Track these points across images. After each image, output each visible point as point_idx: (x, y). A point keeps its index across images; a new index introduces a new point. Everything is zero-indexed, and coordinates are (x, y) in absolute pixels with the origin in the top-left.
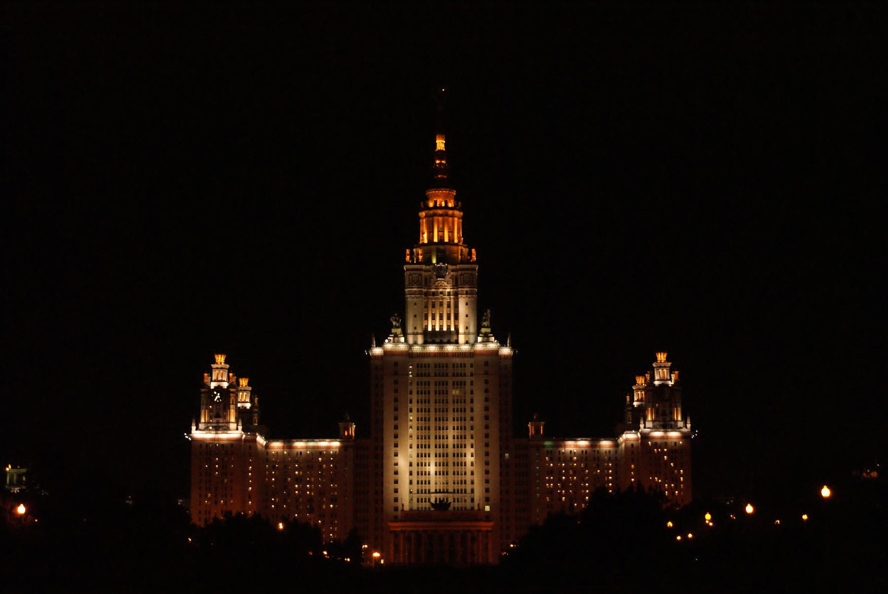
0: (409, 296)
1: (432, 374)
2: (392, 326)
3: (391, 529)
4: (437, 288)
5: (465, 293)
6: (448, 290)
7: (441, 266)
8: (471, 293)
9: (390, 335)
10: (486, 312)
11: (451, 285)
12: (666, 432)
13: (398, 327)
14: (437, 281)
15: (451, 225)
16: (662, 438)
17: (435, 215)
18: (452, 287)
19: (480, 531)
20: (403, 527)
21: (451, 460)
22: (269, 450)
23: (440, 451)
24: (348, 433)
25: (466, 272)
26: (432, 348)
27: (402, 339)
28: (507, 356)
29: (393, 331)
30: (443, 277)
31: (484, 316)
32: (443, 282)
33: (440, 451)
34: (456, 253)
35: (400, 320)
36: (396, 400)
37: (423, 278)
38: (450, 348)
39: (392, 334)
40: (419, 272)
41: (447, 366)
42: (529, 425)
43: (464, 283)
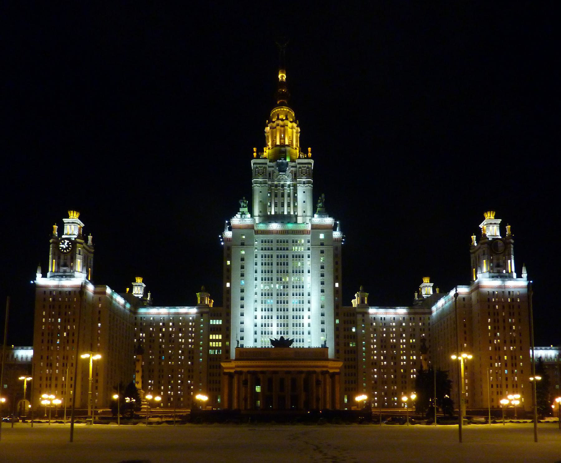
0: (255, 185)
1: (274, 248)
2: (240, 206)
3: (226, 371)
4: (279, 180)
5: (303, 183)
6: (288, 183)
7: (282, 162)
8: (309, 182)
9: (238, 213)
10: (321, 196)
11: (291, 178)
12: (503, 281)
13: (245, 207)
14: (278, 175)
15: (290, 135)
16: (500, 287)
17: (278, 125)
18: (291, 180)
19: (327, 372)
21: (291, 321)
23: (281, 313)
25: (304, 165)
27: (249, 215)
29: (241, 210)
30: (285, 171)
32: (284, 176)
33: (281, 313)
35: (247, 202)
36: (242, 267)
38: (290, 226)
39: (239, 212)
40: (264, 166)
43: (302, 174)
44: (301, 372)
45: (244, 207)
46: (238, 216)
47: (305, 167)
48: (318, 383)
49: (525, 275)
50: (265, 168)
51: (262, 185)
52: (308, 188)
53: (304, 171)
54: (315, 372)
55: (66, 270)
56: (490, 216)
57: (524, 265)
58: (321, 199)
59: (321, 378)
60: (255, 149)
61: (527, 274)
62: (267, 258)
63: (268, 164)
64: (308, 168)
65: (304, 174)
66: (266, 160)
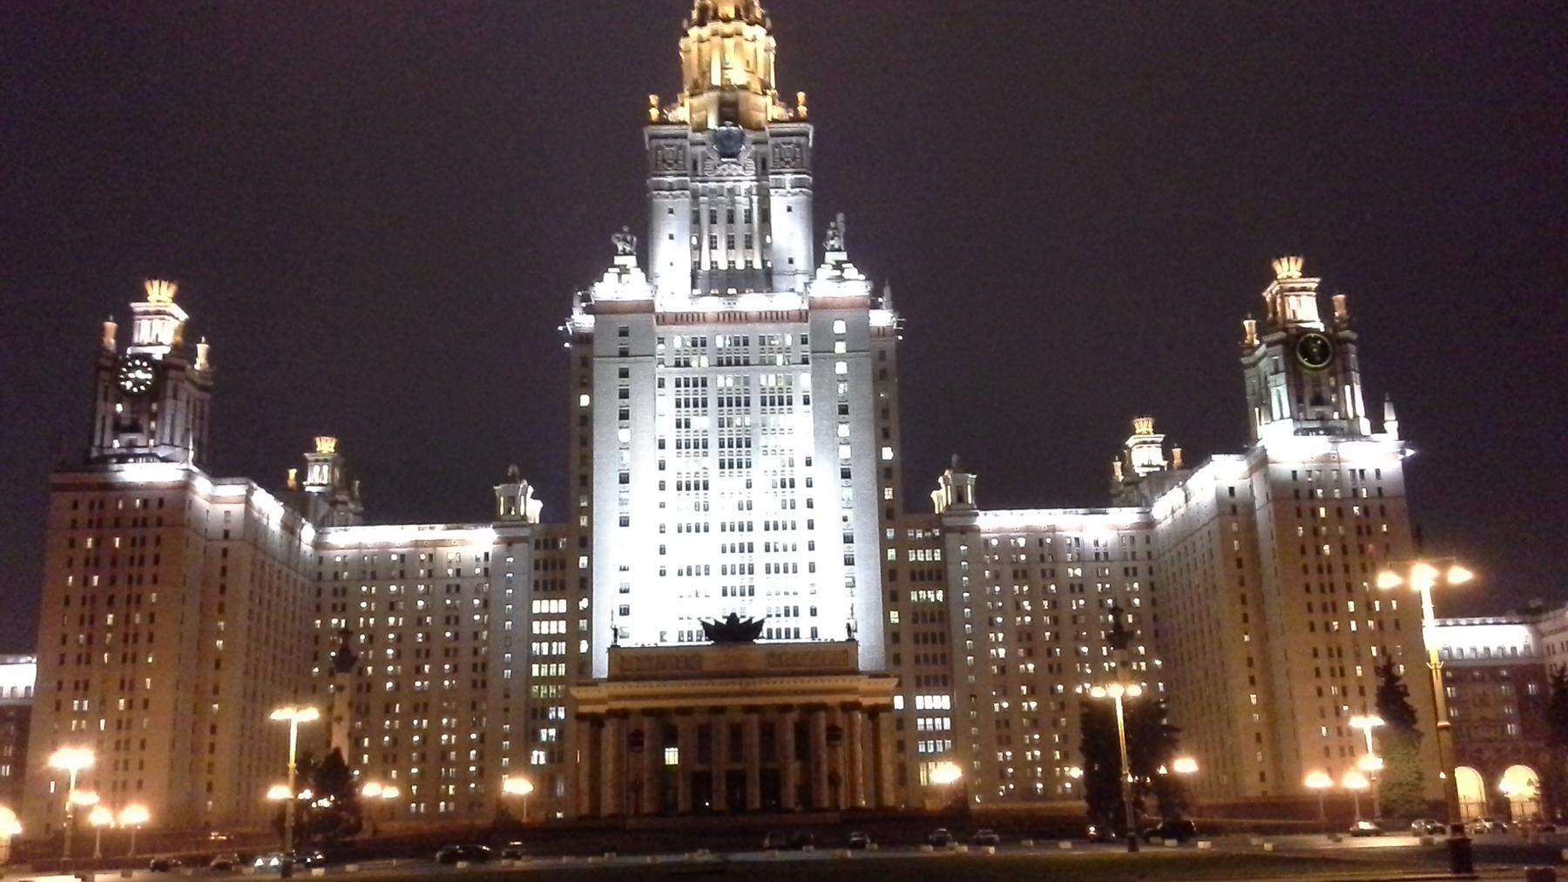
0: (655, 193)
3: (584, 709)
9: (610, 270)
10: (834, 220)
11: (753, 172)
13: (630, 254)
14: (718, 165)
16: (1327, 459)
18: (754, 178)
19: (857, 706)
20: (619, 698)
22: (324, 553)
24: (518, 512)
26: (712, 305)
28: (884, 328)
29: (618, 260)
31: (828, 227)
32: (734, 166)
34: (760, 111)
35: (635, 239)
37: (689, 159)
40: (678, 142)
41: (746, 343)
42: (934, 495)
43: (784, 163)
44: (787, 708)
45: (625, 253)
46: (610, 276)
47: (790, 144)
48: (834, 733)
49: (1391, 424)
50: (681, 147)
51: (673, 193)
52: (795, 198)
53: (788, 154)
54: (822, 707)
55: (136, 440)
56: (1288, 269)
57: (1387, 399)
58: (836, 228)
59: (841, 720)
60: (653, 99)
61: (1396, 422)
62: (691, 389)
63: (689, 137)
64: (798, 145)
65: (788, 163)
66: (684, 127)
